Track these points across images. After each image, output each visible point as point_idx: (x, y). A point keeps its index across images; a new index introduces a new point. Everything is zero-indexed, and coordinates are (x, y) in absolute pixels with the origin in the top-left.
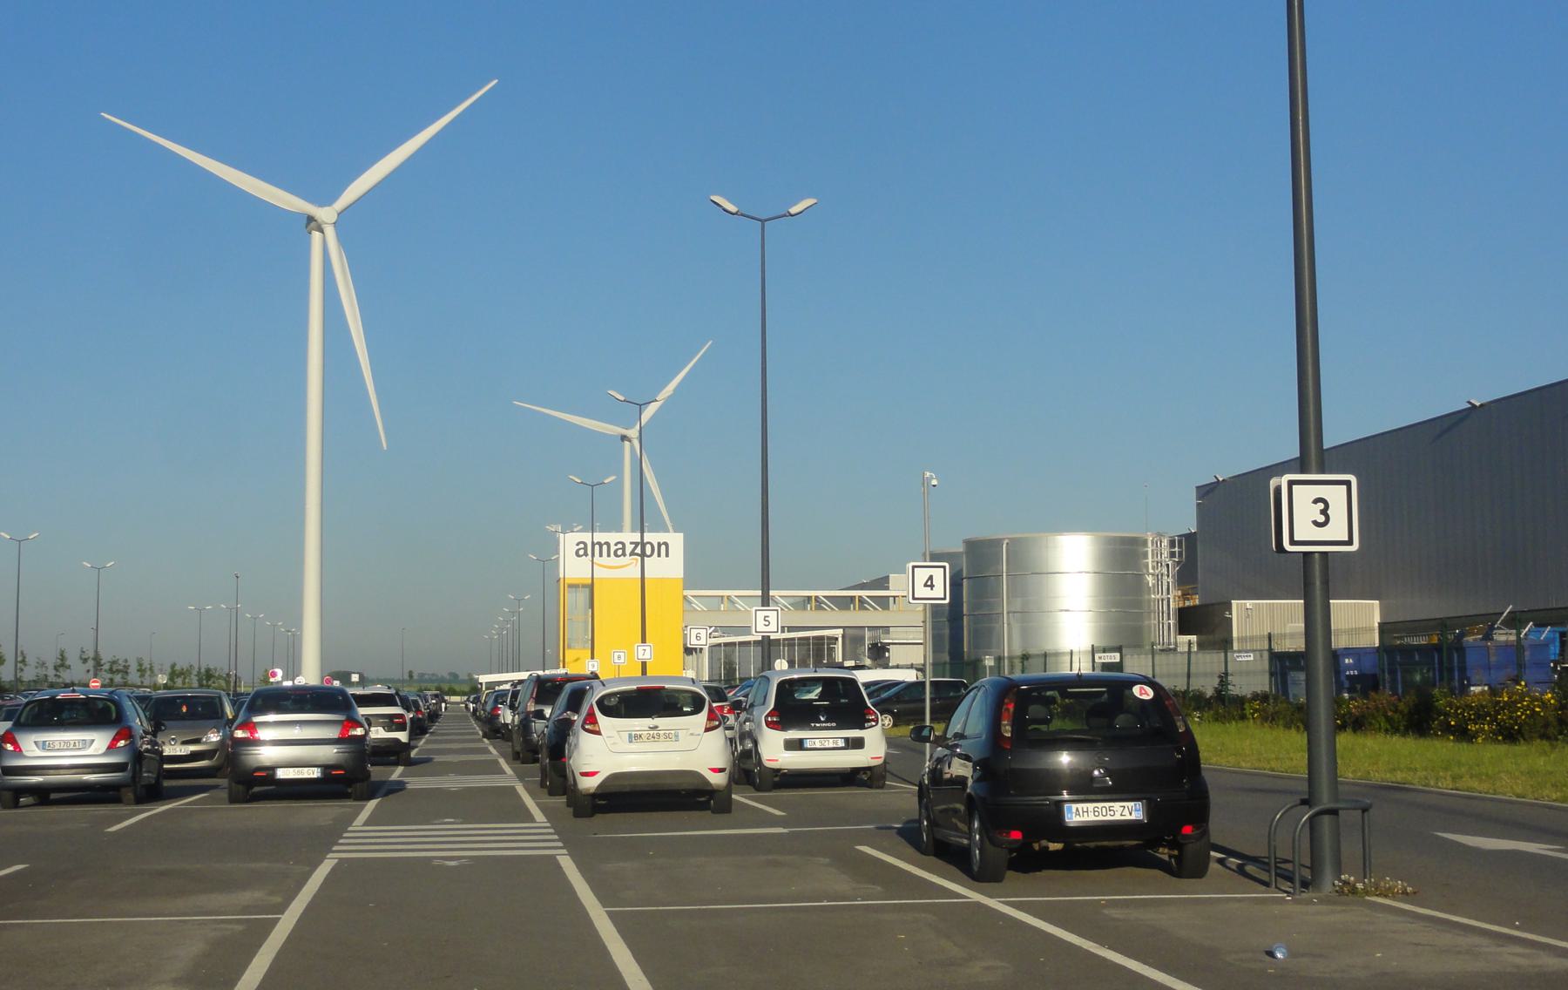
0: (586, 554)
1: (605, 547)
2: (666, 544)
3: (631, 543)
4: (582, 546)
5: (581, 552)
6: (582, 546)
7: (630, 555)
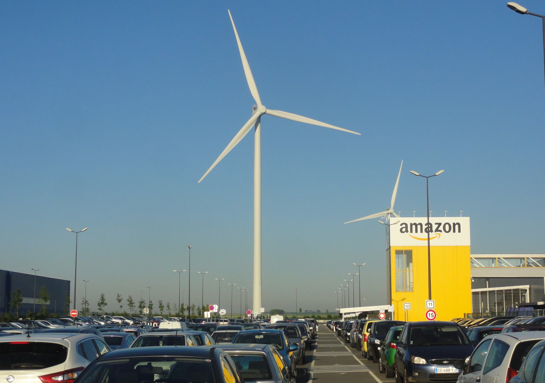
0: (407, 231)
1: (419, 227)
2: (459, 224)
3: (436, 224)
4: (404, 226)
5: (404, 230)
6: (404, 226)
7: (435, 232)
